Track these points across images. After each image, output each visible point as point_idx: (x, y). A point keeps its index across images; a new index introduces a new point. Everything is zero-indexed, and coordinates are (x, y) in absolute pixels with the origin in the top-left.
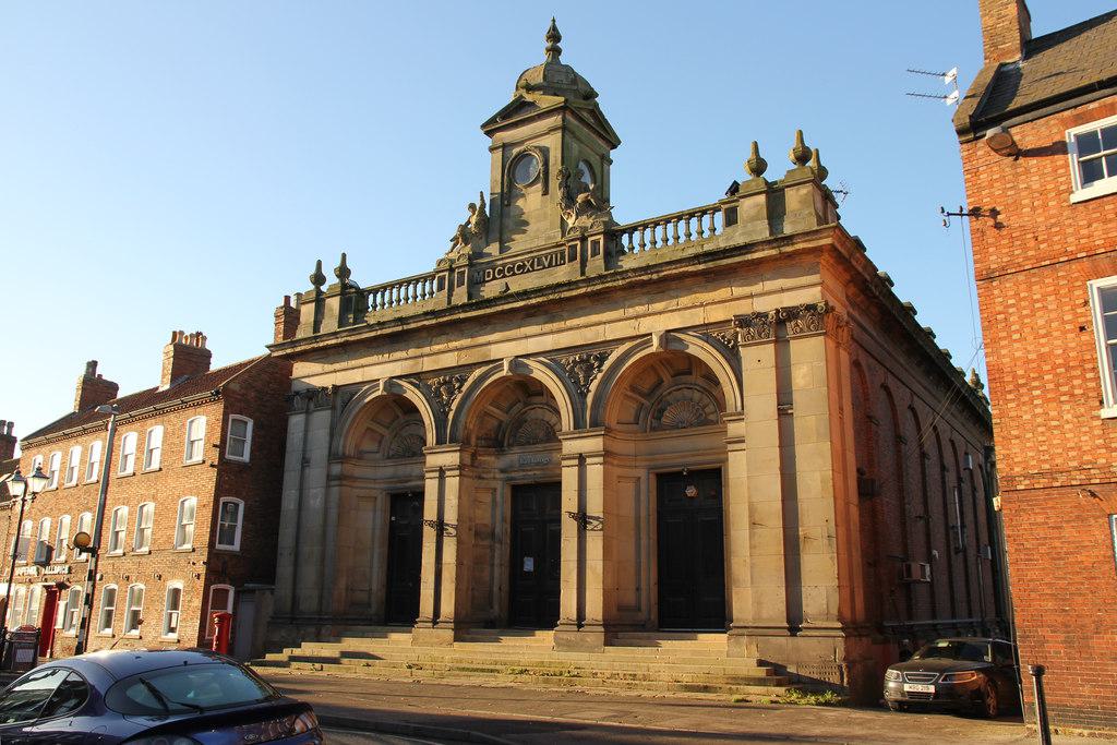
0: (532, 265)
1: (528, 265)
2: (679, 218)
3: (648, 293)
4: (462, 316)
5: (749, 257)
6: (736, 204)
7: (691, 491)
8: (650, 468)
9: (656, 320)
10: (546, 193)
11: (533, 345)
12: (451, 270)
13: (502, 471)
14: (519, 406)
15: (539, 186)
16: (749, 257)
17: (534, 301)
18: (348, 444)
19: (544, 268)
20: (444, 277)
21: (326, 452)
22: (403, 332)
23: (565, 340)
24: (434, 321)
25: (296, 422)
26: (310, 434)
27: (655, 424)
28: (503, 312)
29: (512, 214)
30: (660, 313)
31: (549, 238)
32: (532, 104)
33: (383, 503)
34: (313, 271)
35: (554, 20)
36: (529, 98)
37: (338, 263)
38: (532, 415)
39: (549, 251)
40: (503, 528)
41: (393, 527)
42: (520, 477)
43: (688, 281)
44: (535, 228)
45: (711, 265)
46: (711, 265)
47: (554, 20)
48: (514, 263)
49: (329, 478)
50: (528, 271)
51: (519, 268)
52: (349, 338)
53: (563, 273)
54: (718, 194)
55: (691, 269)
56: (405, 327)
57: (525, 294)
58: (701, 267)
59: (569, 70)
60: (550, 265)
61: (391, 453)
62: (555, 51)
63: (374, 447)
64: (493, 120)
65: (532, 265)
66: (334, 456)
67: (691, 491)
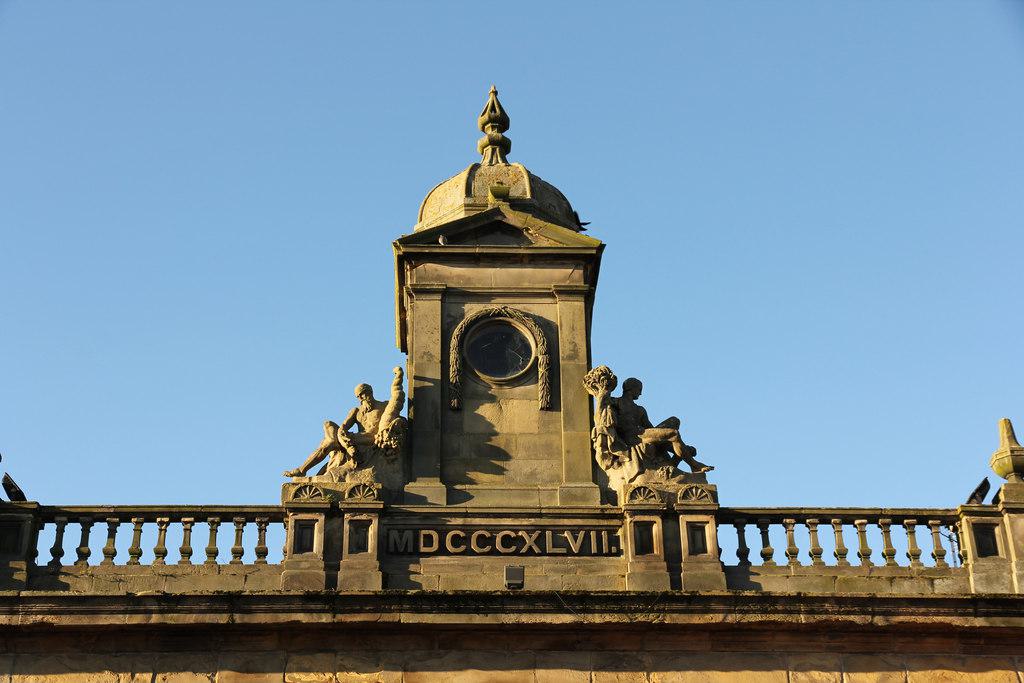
0: (540, 541)
1: (529, 541)
2: (824, 518)
3: (840, 650)
4: (407, 618)
6: (994, 520)
10: (552, 404)
12: (333, 513)
17: (597, 619)
19: (570, 553)
20: (310, 525)
22: (229, 629)
24: (325, 618)
28: (502, 628)
29: (466, 429)
31: (574, 497)
32: (516, 233)
36: (514, 218)
39: (579, 522)
43: (931, 642)
44: (527, 470)
45: (999, 622)
46: (999, 622)
48: (495, 529)
50: (530, 552)
51: (506, 541)
52: (50, 619)
53: (623, 573)
54: (953, 497)
55: (957, 621)
56: (238, 618)
58: (979, 622)
60: (584, 550)
64: (429, 236)
65: (540, 541)
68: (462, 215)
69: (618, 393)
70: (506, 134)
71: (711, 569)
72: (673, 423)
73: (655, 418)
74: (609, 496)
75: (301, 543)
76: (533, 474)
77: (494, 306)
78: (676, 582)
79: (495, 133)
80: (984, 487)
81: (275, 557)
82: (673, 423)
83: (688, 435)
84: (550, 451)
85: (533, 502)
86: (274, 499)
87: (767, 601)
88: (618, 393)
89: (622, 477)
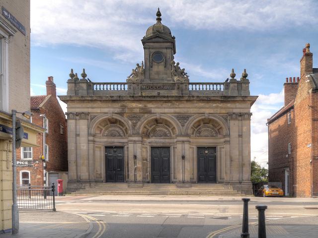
5: (235, 99)
7: (206, 152)
8: (196, 146)
9: (208, 110)
11: (166, 110)
13: (149, 143)
14: (154, 126)
15: (163, 63)
16: (235, 99)
18: (92, 131)
20: (131, 85)
21: (86, 133)
23: (177, 110)
25: (71, 124)
26: (78, 127)
27: (198, 135)
30: (208, 108)
33: (103, 149)
34: (70, 73)
35: (159, 9)
37: (82, 72)
38: (158, 129)
40: (149, 158)
41: (106, 156)
42: (155, 145)
47: (159, 9)
49: (89, 141)
53: (175, 93)
57: (164, 97)
59: (165, 28)
61: (106, 135)
62: (159, 20)
63: (99, 132)
66: (89, 134)
67: (206, 152)
68: (152, 35)
69: (176, 65)
70: (161, 17)
71: (187, 92)
72: (184, 69)
73: (181, 69)
74: (174, 81)
75: (129, 88)
76: (163, 77)
77: (157, 50)
78: (182, 94)
79: (161, 17)
80: (228, 79)
81: (126, 89)
82: (184, 69)
83: (185, 72)
84: (166, 74)
85: (163, 82)
86: (126, 82)
87: (193, 97)
88: (176, 65)
89: (176, 78)
